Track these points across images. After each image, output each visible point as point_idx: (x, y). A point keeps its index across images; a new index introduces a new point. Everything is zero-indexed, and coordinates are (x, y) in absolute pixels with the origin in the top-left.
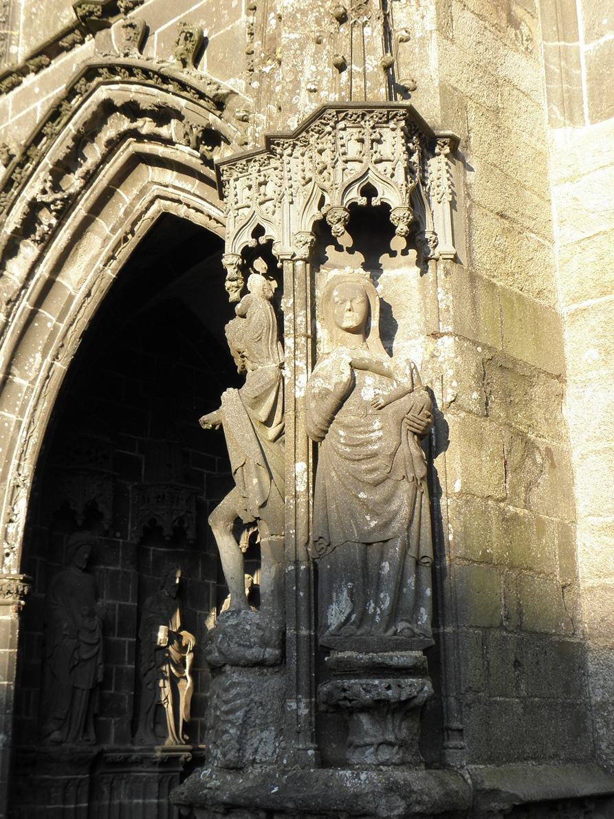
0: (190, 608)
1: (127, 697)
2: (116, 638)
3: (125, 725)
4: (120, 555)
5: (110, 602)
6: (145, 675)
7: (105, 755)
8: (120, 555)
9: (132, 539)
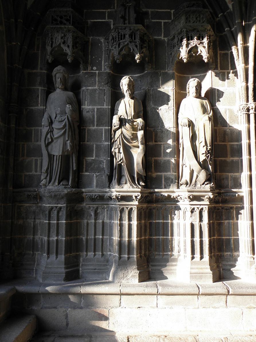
0: (153, 106)
4: (97, 80)
5: (90, 107)
8: (97, 80)
9: (105, 69)
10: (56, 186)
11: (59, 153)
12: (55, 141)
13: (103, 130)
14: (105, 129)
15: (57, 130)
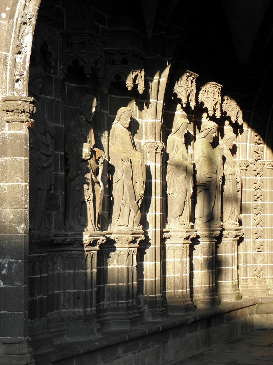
3: (60, 217)
4: (54, 87)
8: (54, 87)
9: (60, 76)
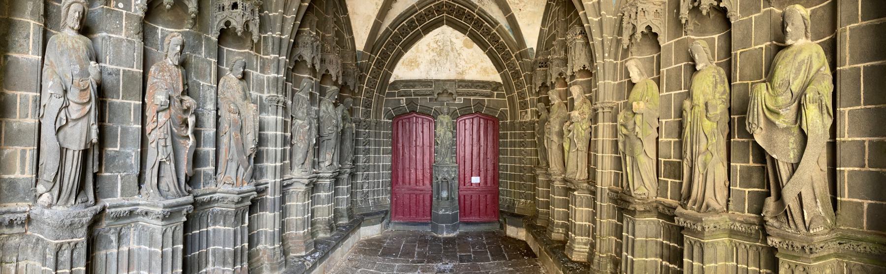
1: (133, 154)
2: (120, 101)
6: (150, 134)
7: (107, 211)
10: (72, 205)
11: (80, 146)
12: (70, 124)
13: (132, 106)
14: (134, 104)
15: (77, 105)
